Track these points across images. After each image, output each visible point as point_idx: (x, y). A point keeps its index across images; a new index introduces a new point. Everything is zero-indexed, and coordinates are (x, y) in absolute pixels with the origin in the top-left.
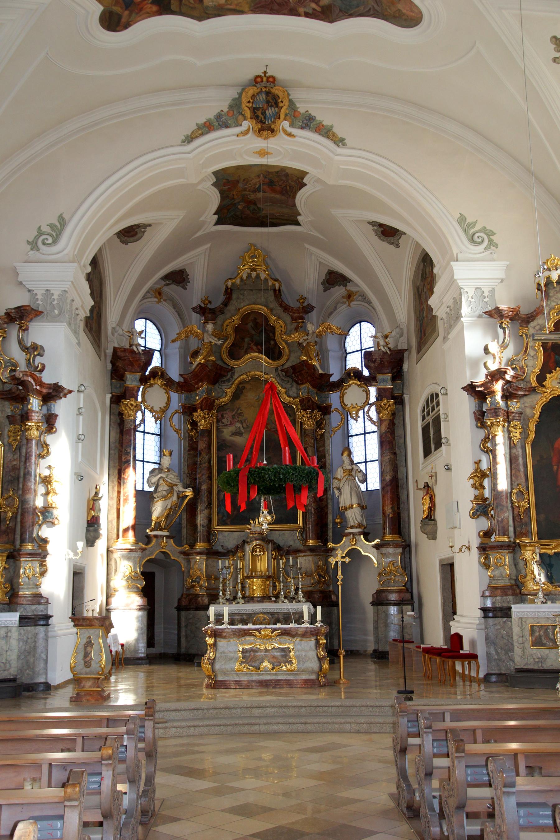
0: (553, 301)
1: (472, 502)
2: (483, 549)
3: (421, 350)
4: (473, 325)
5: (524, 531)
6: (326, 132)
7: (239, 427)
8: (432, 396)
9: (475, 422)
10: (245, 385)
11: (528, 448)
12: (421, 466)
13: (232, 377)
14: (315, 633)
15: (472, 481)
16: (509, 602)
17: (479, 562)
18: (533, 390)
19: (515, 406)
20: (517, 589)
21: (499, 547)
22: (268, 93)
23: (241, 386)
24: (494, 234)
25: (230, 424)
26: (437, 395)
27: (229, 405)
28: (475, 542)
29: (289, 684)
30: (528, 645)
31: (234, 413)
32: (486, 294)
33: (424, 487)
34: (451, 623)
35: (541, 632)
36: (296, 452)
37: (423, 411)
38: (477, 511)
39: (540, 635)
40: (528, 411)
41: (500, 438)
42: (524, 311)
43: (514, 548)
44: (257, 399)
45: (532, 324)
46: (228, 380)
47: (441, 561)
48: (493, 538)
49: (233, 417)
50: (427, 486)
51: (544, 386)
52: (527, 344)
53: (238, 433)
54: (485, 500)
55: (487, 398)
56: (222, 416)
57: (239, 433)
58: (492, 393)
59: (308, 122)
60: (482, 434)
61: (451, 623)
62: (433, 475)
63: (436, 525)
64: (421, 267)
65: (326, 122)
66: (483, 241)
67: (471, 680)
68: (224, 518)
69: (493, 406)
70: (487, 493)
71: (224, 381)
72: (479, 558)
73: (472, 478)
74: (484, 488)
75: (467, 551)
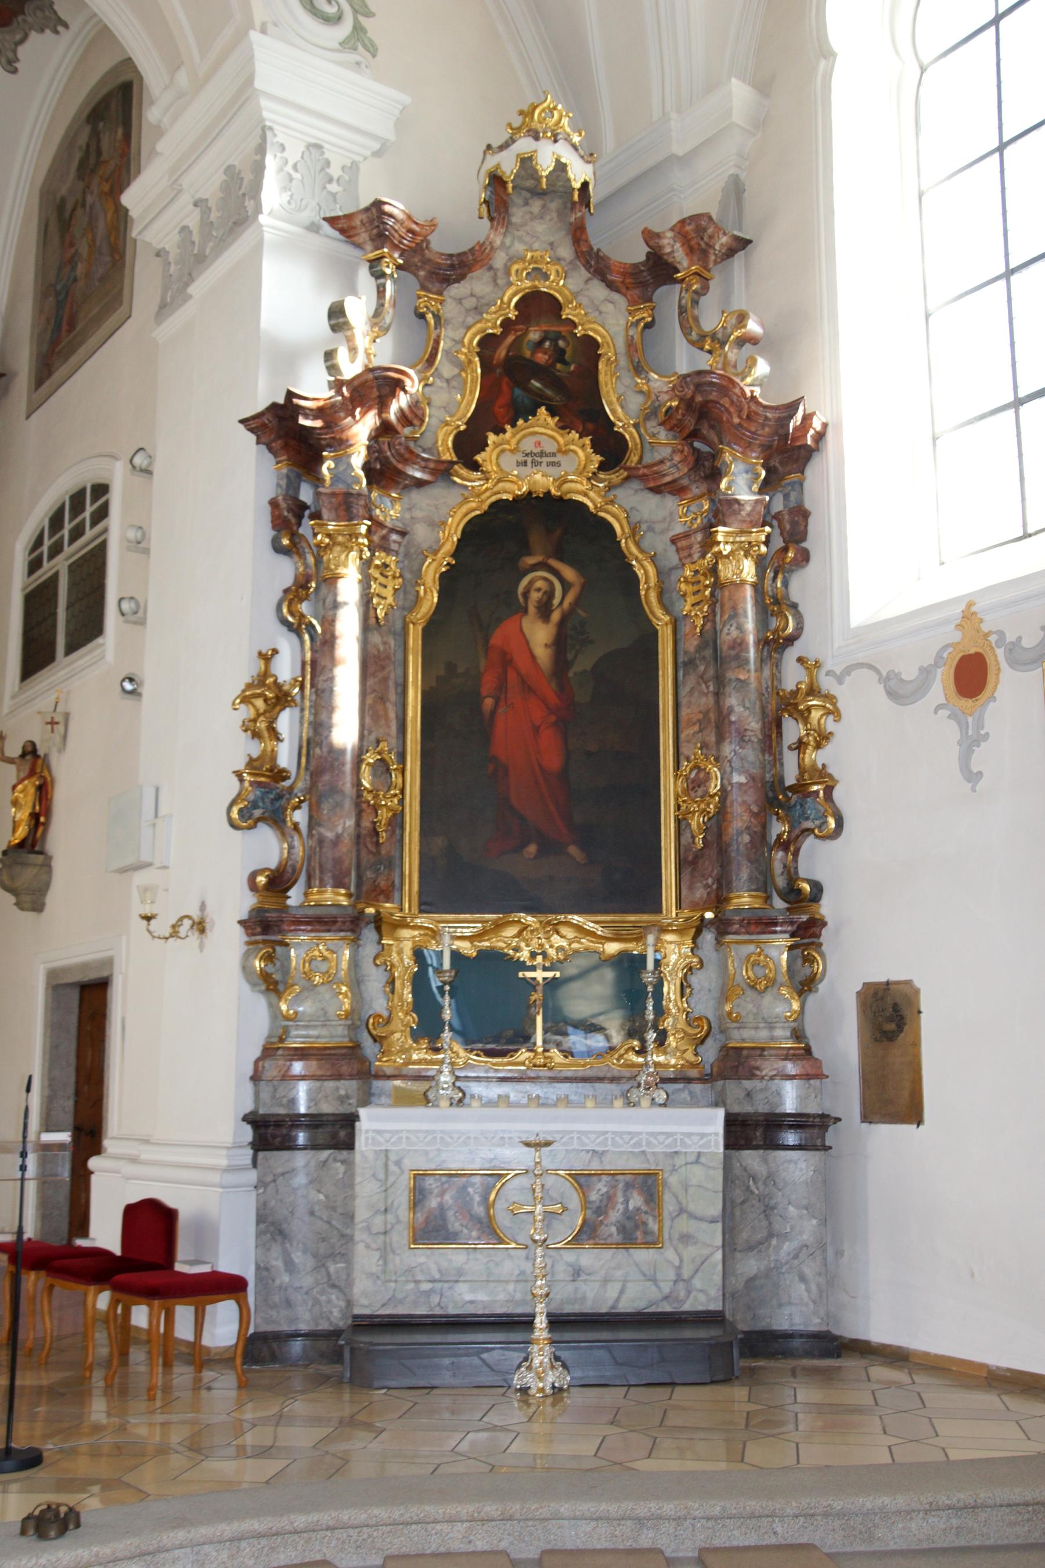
0: (521, 240)
1: (239, 775)
2: (266, 926)
3: (50, 374)
5: (382, 883)
8: (77, 500)
9: (269, 533)
12: (7, 702)
15: (245, 712)
16: (343, 1099)
17: (246, 969)
18: (442, 472)
19: (391, 509)
24: (369, 14)
26: (101, 490)
30: (401, 1237)
32: (335, 171)
33: (23, 755)
34: (93, 1163)
35: (447, 1197)
37: (39, 542)
38: (254, 805)
39: (442, 1208)
40: (421, 533)
41: (349, 588)
42: (441, 244)
45: (456, 290)
47: (52, 974)
48: (295, 897)
50: (30, 752)
51: (475, 467)
52: (437, 342)
54: (281, 775)
55: (321, 460)
58: (341, 444)
60: (284, 572)
61: (93, 1163)
62: (58, 723)
63: (47, 866)
64: (83, 139)
66: (338, 19)
67: (198, 1357)
69: (341, 488)
70: (286, 757)
72: (247, 956)
73: (245, 700)
74: (276, 736)
75: (194, 938)
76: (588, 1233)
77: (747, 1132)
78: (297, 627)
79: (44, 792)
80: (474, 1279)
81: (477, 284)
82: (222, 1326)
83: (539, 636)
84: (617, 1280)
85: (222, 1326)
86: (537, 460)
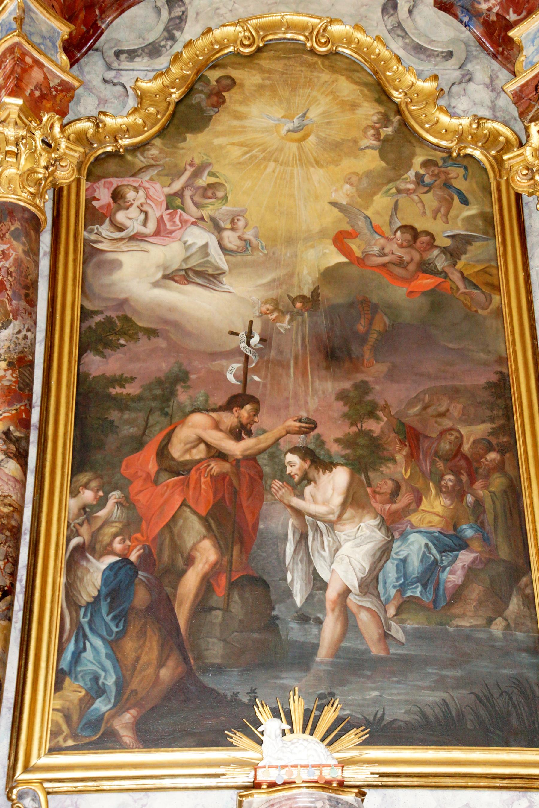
7: (206, 246)
10: (235, 73)
13: (172, 38)
23: (213, 75)
25: (157, 233)
27: (154, 152)
31: (177, 186)
36: (503, 360)
44: (294, 131)
46: (153, 50)
49: (173, 202)
53: (197, 273)
56: (117, 195)
57: (199, 274)
68: (101, 706)
71: (132, 54)
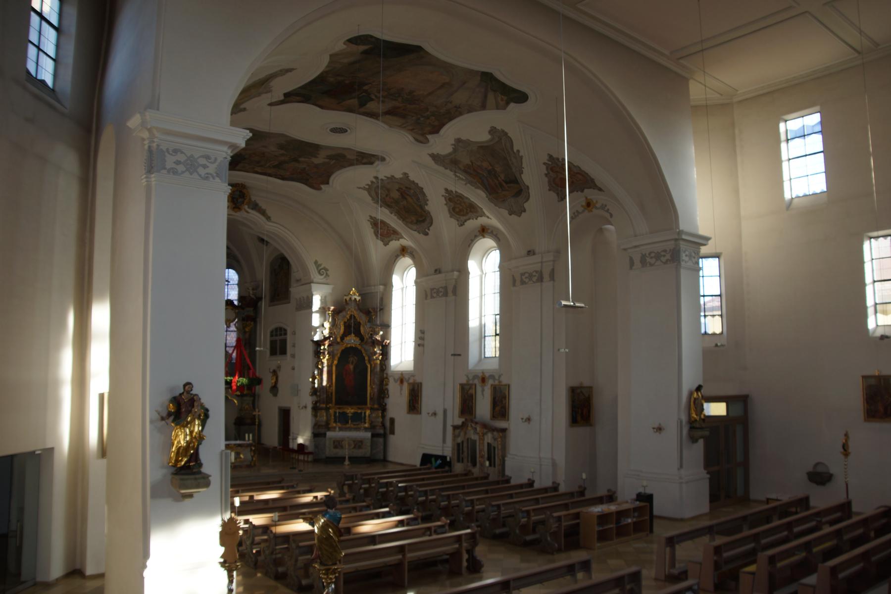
4: (317, 312)
6: (263, 212)
11: (334, 368)
14: (250, 445)
20: (327, 426)
21: (322, 409)
22: (241, 192)
28: (310, 406)
29: (241, 467)
43: (327, 409)
58: (324, 345)
59: (255, 207)
60: (316, 360)
65: (264, 207)
76: (354, 447)
77: (373, 436)
78: (317, 367)
79: (277, 378)
80: (340, 452)
81: (344, 313)
82: (310, 458)
83: (351, 367)
84: (359, 453)
85: (310, 458)
86: (352, 340)
